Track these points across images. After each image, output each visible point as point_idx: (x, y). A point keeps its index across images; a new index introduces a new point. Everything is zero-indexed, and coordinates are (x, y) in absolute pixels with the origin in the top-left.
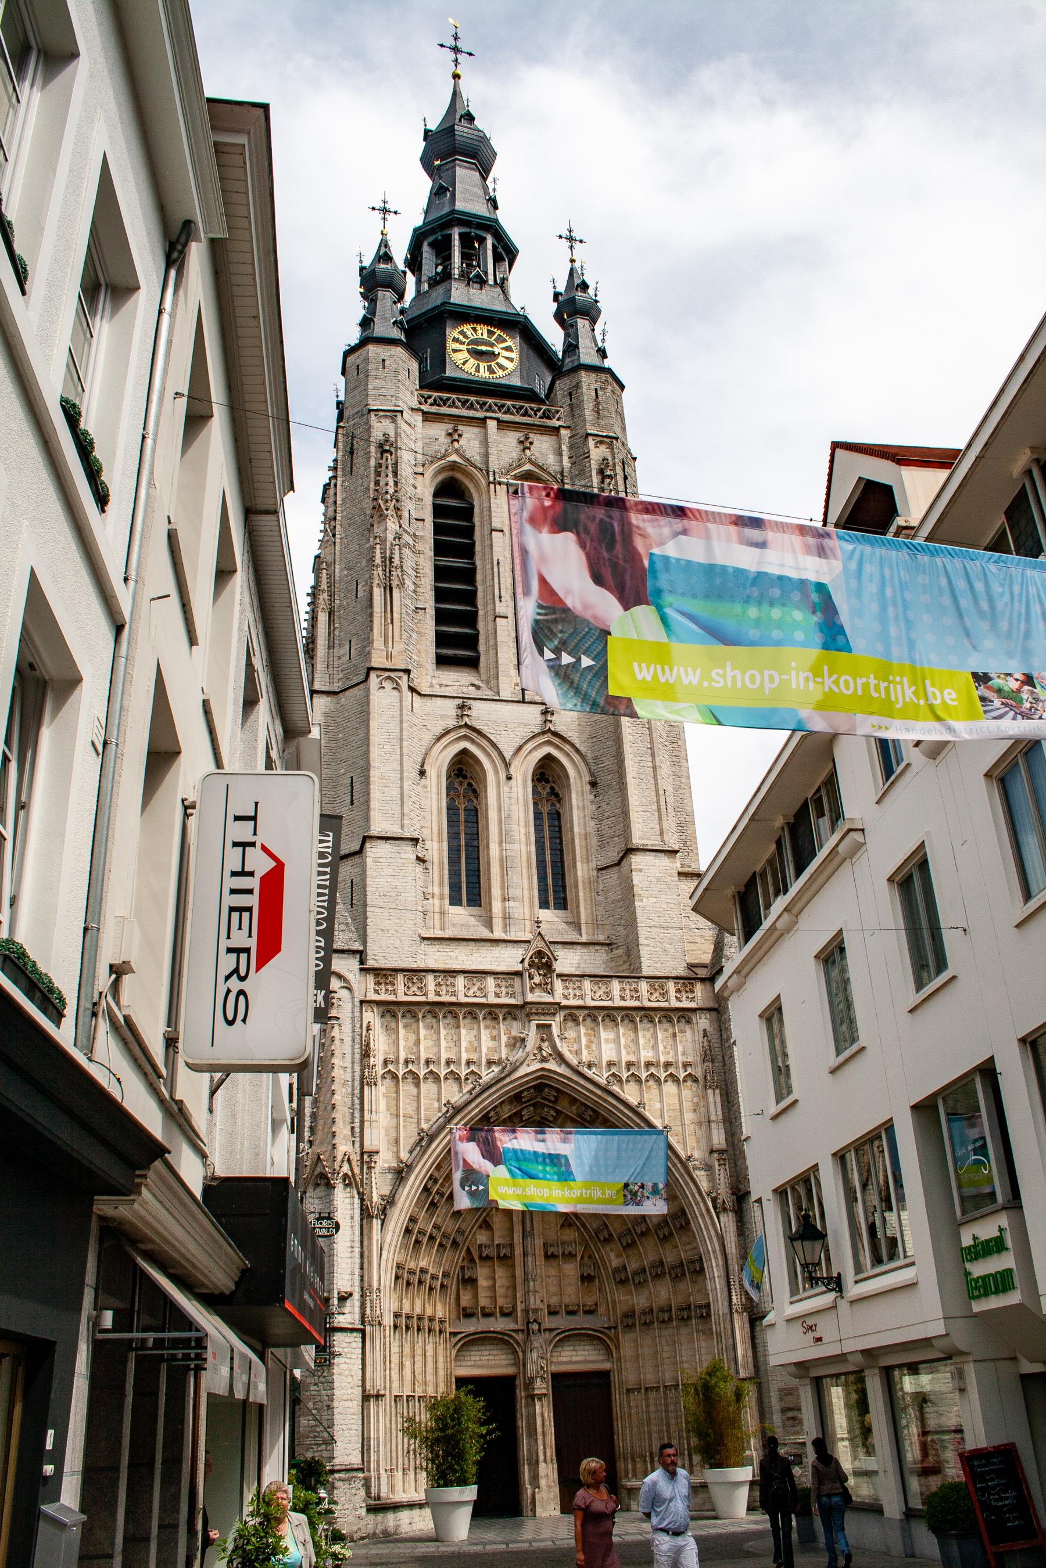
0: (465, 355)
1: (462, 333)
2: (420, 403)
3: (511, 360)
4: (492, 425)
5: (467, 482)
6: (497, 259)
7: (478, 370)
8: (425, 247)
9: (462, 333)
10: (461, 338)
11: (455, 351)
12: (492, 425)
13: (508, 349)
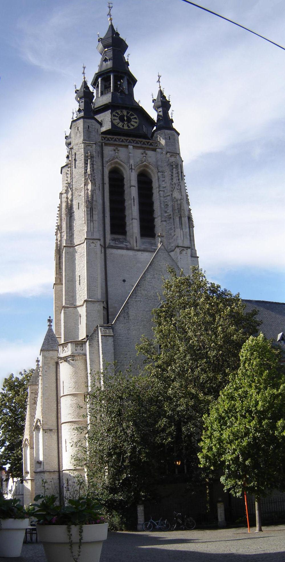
0: (118, 121)
2: (102, 140)
3: (136, 122)
4: (131, 147)
5: (122, 169)
7: (123, 126)
8: (100, 80)
12: (131, 147)
13: (135, 118)
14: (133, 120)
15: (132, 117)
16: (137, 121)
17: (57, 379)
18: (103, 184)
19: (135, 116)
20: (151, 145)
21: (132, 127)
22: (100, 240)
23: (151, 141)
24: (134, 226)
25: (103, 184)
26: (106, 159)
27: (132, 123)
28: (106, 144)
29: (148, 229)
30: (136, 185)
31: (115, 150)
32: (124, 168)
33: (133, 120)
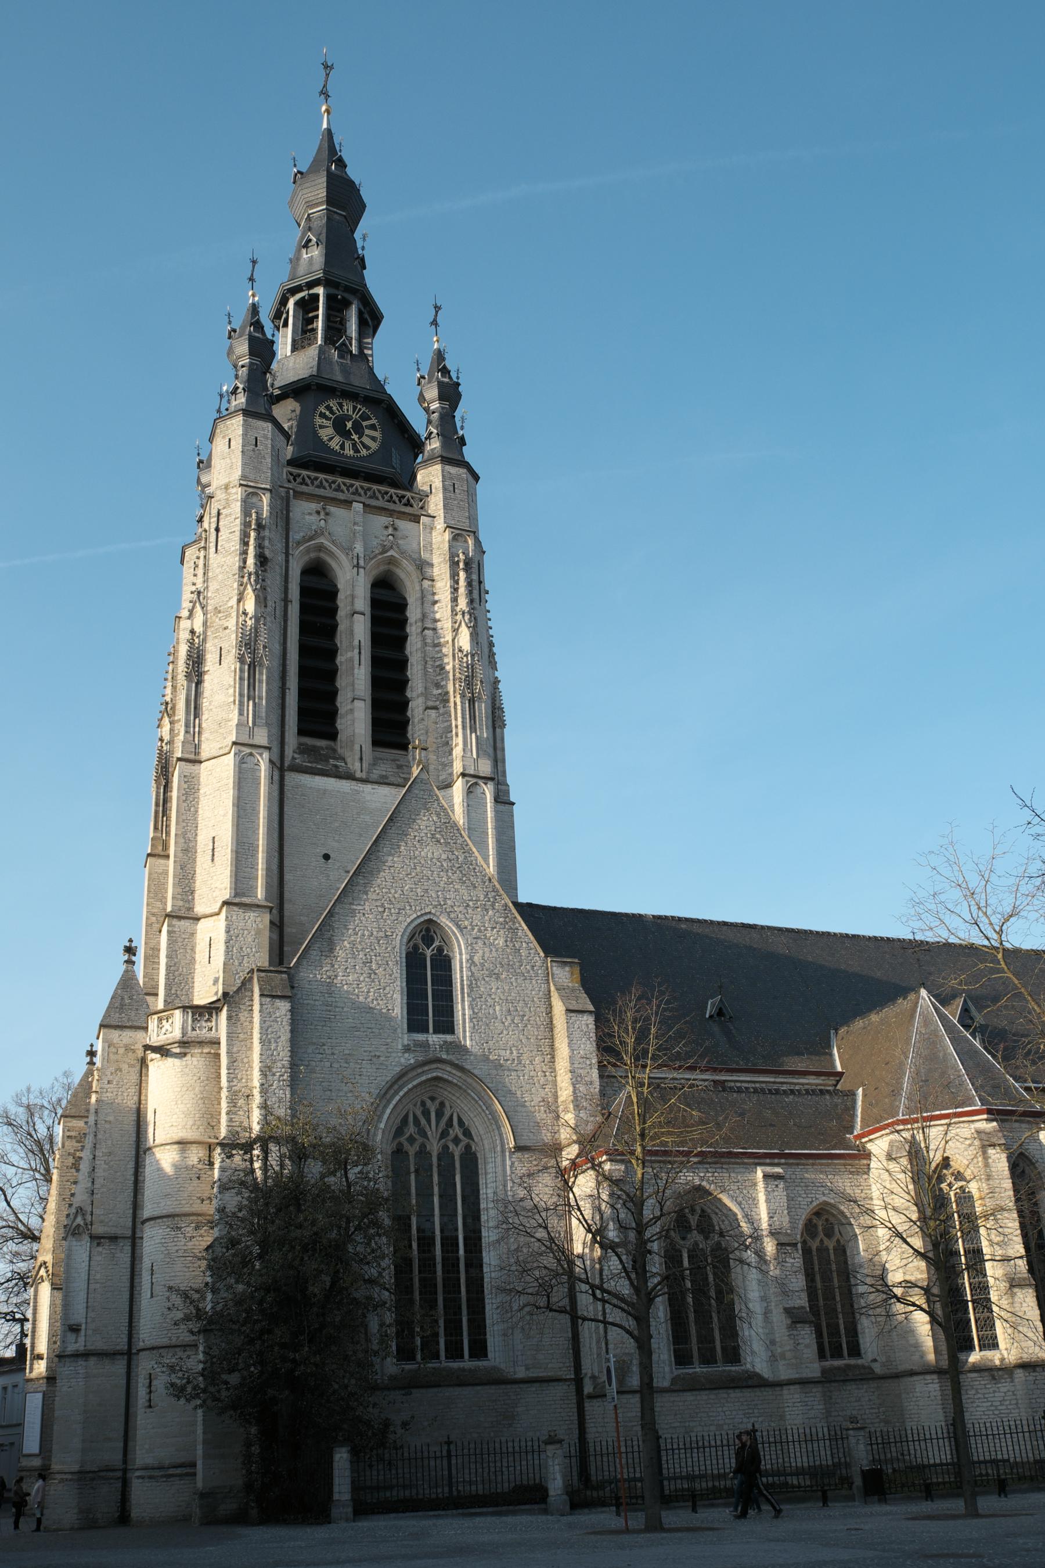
0: (330, 431)
1: (329, 408)
3: (374, 439)
4: (358, 507)
5: (333, 564)
6: (362, 323)
7: (342, 447)
8: (291, 304)
9: (329, 408)
10: (327, 413)
11: (321, 427)
12: (358, 507)
13: (373, 427)
14: (367, 432)
15: (364, 424)
16: (377, 434)
17: (136, 1182)
18: (286, 601)
19: (374, 421)
20: (408, 504)
21: (364, 452)
22: (269, 748)
23: (408, 494)
24: (356, 718)
25: (286, 601)
26: (295, 536)
27: (365, 439)
28: (298, 495)
29: (391, 728)
30: (368, 611)
31: (318, 513)
32: (340, 564)
33: (367, 432)
